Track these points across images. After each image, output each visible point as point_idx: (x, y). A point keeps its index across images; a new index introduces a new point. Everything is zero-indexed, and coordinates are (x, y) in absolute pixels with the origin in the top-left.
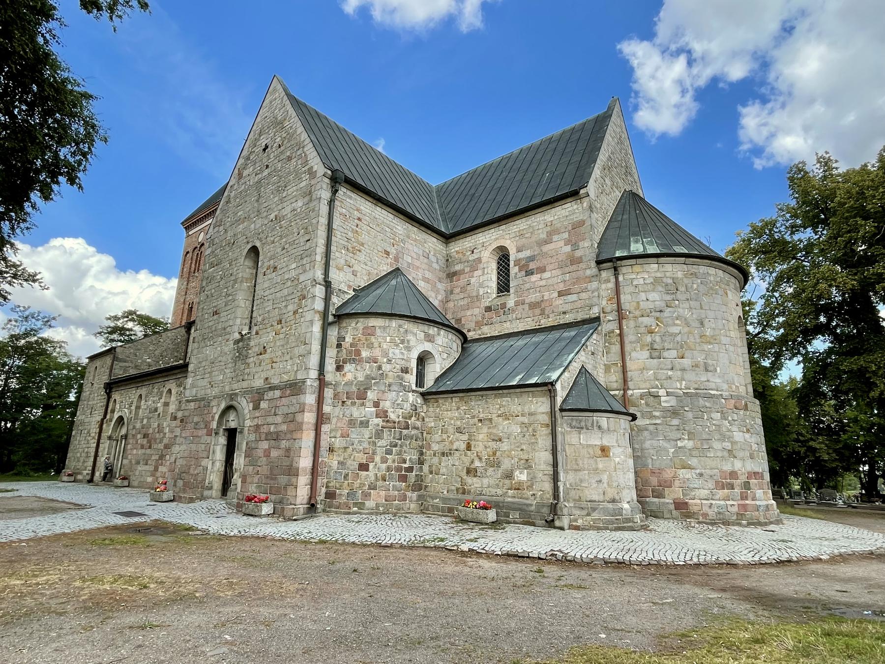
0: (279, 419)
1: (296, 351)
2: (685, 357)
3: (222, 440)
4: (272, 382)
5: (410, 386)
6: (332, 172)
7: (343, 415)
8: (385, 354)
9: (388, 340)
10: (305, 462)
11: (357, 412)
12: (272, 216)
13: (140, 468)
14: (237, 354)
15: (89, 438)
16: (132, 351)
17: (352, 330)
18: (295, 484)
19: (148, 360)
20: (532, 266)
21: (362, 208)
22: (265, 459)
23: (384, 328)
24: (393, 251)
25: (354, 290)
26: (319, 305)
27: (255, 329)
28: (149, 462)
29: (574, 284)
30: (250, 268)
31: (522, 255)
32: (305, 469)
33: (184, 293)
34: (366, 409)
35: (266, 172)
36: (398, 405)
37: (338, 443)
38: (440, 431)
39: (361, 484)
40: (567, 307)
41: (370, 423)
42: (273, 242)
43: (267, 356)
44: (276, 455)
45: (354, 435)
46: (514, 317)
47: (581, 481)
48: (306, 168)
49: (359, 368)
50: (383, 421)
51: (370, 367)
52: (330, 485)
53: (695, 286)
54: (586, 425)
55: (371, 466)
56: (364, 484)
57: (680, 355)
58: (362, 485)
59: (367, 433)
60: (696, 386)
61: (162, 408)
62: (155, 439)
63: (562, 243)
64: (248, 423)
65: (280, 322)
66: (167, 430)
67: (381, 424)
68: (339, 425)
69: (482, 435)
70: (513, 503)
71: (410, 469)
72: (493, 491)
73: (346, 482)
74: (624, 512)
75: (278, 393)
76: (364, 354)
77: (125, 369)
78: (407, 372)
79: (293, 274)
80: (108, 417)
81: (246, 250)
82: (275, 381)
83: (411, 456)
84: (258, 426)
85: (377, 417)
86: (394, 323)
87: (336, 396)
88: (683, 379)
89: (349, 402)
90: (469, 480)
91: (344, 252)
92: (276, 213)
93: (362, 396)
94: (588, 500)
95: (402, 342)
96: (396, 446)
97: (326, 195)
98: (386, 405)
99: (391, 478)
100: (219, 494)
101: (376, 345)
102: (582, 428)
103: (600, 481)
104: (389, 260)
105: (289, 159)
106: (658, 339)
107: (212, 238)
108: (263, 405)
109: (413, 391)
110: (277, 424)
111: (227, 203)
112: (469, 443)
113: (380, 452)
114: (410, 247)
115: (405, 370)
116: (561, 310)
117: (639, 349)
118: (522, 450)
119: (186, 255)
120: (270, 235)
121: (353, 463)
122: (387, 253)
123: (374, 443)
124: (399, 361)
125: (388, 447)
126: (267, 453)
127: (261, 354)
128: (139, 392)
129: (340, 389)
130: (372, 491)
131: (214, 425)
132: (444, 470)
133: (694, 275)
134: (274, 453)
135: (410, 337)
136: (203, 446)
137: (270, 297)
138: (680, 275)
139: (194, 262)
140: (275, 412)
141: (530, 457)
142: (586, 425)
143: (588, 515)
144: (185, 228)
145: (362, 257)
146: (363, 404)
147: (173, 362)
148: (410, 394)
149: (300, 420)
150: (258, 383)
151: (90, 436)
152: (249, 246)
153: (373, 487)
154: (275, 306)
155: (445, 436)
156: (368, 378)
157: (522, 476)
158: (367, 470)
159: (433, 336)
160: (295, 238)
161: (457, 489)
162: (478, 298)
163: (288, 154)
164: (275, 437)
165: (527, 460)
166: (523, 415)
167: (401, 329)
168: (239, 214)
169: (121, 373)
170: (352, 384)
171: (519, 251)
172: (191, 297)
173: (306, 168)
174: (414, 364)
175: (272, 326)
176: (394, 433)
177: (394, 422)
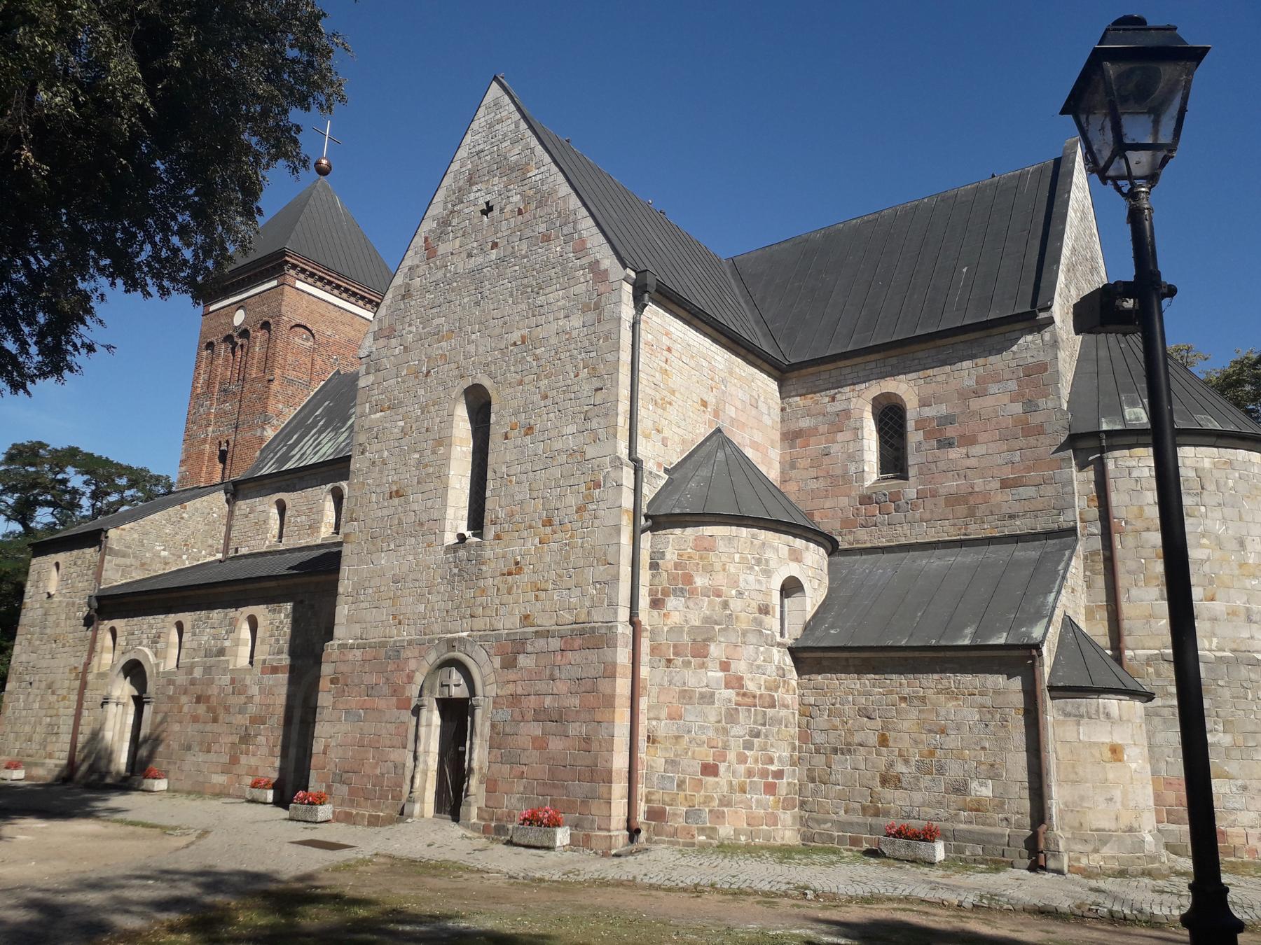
0: (561, 687)
1: (589, 574)
2: (1217, 596)
5: (773, 636)
6: (636, 273)
7: (670, 682)
8: (736, 583)
9: (737, 560)
10: (620, 762)
11: (694, 679)
12: (516, 336)
14: (456, 571)
16: (136, 536)
17: (677, 541)
18: (606, 796)
19: (164, 553)
20: (950, 432)
21: (672, 329)
22: (536, 753)
23: (730, 539)
24: (711, 399)
25: (666, 470)
26: (627, 501)
29: (1028, 469)
31: (928, 412)
32: (620, 770)
34: (709, 673)
35: (494, 254)
36: (759, 667)
37: (664, 728)
38: (826, 713)
39: (706, 797)
40: (1017, 508)
41: (717, 696)
42: (520, 383)
43: (523, 578)
44: (561, 747)
45: (692, 716)
46: (918, 516)
47: (1082, 798)
48: (585, 261)
49: (691, 604)
50: (738, 694)
51: (709, 603)
52: (653, 797)
53: (1231, 483)
54: (1087, 712)
55: (722, 768)
56: (712, 798)
57: (1209, 594)
58: (708, 799)
60: (1234, 646)
63: (1006, 399)
65: (548, 522)
66: (255, 690)
67: (734, 698)
68: (662, 699)
69: (908, 723)
70: (969, 832)
71: (779, 774)
72: (932, 812)
73: (682, 794)
74: (1147, 847)
75: (555, 643)
76: (700, 581)
77: (125, 569)
78: (767, 613)
79: (571, 443)
82: (546, 622)
84: (515, 699)
85: (727, 687)
86: (744, 531)
87: (654, 650)
88: (1214, 635)
89: (679, 661)
90: (888, 793)
91: (651, 408)
92: (523, 332)
93: (700, 652)
94: (1094, 827)
95: (758, 562)
96: (758, 735)
97: (627, 311)
98: (740, 667)
99: (754, 789)
100: (439, 808)
101: (718, 566)
102: (1082, 716)
103: (1111, 799)
105: (546, 238)
107: (373, 357)
108: (522, 660)
109: (779, 645)
110: (561, 694)
111: (403, 297)
112: (883, 735)
113: (735, 746)
115: (765, 610)
116: (1006, 510)
117: (1142, 583)
118: (983, 748)
120: (512, 368)
121: (692, 762)
122: (704, 404)
123: (725, 731)
124: (754, 595)
125: (747, 737)
126: (540, 744)
127: (510, 574)
129: (662, 639)
130: (726, 809)
132: (839, 777)
133: (1230, 464)
134: (555, 744)
135: (769, 554)
136: (392, 728)
138: (1207, 463)
140: (551, 675)
141: (998, 760)
142: (1087, 712)
143: (1096, 851)
145: (672, 413)
146: (703, 666)
147: (205, 557)
148: (775, 650)
149: (608, 691)
150: (508, 623)
152: (468, 382)
153: (726, 803)
154: (535, 494)
155: (837, 722)
156: (707, 623)
157: (983, 790)
158: (716, 774)
159: (801, 552)
161: (864, 809)
162: (846, 478)
163: (542, 228)
164: (555, 716)
165: (992, 766)
166: (981, 694)
167: (756, 542)
168: (435, 322)
170: (682, 632)
171: (924, 403)
173: (585, 261)
175: (531, 527)
176: (755, 715)
177: (754, 697)
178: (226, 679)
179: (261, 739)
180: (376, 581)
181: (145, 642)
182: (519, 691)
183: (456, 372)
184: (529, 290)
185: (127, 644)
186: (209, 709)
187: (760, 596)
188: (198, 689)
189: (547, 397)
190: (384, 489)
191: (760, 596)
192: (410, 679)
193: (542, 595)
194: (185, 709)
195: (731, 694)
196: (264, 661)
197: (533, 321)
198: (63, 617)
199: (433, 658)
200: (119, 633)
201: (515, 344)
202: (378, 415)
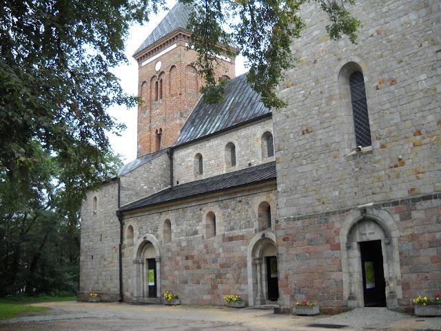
3: (356, 253)
4: (422, 192)
13: (188, 288)
15: (106, 263)
27: (376, 144)
28: (201, 281)
30: (344, 84)
33: (148, 122)
42: (381, 56)
61: (204, 231)
62: (205, 261)
64: (395, 234)
65: (419, 133)
66: (221, 250)
77: (129, 196)
79: (425, 85)
80: (126, 242)
81: (339, 68)
84: (413, 237)
92: (377, 28)
108: (415, 214)
119: (142, 86)
127: (396, 166)
128: (164, 217)
131: (343, 239)
136: (329, 261)
137: (393, 110)
139: (154, 90)
144: (138, 60)
147: (163, 188)
151: (105, 260)
152: (343, 63)
154: (404, 118)
160: (416, 50)
169: (127, 200)
172: (156, 125)
178: (202, 246)
179: (229, 275)
180: (303, 182)
181: (150, 231)
182: (416, 232)
183: (334, 58)
184: (376, 5)
185: (140, 233)
186: (194, 262)
188: (186, 253)
189: (402, 61)
190: (296, 130)
192: (337, 233)
193: (420, 175)
194: (180, 263)
196: (224, 235)
197: (382, 21)
198: (103, 223)
199: (351, 219)
200: (134, 229)
201: (372, 35)
202: (286, 90)
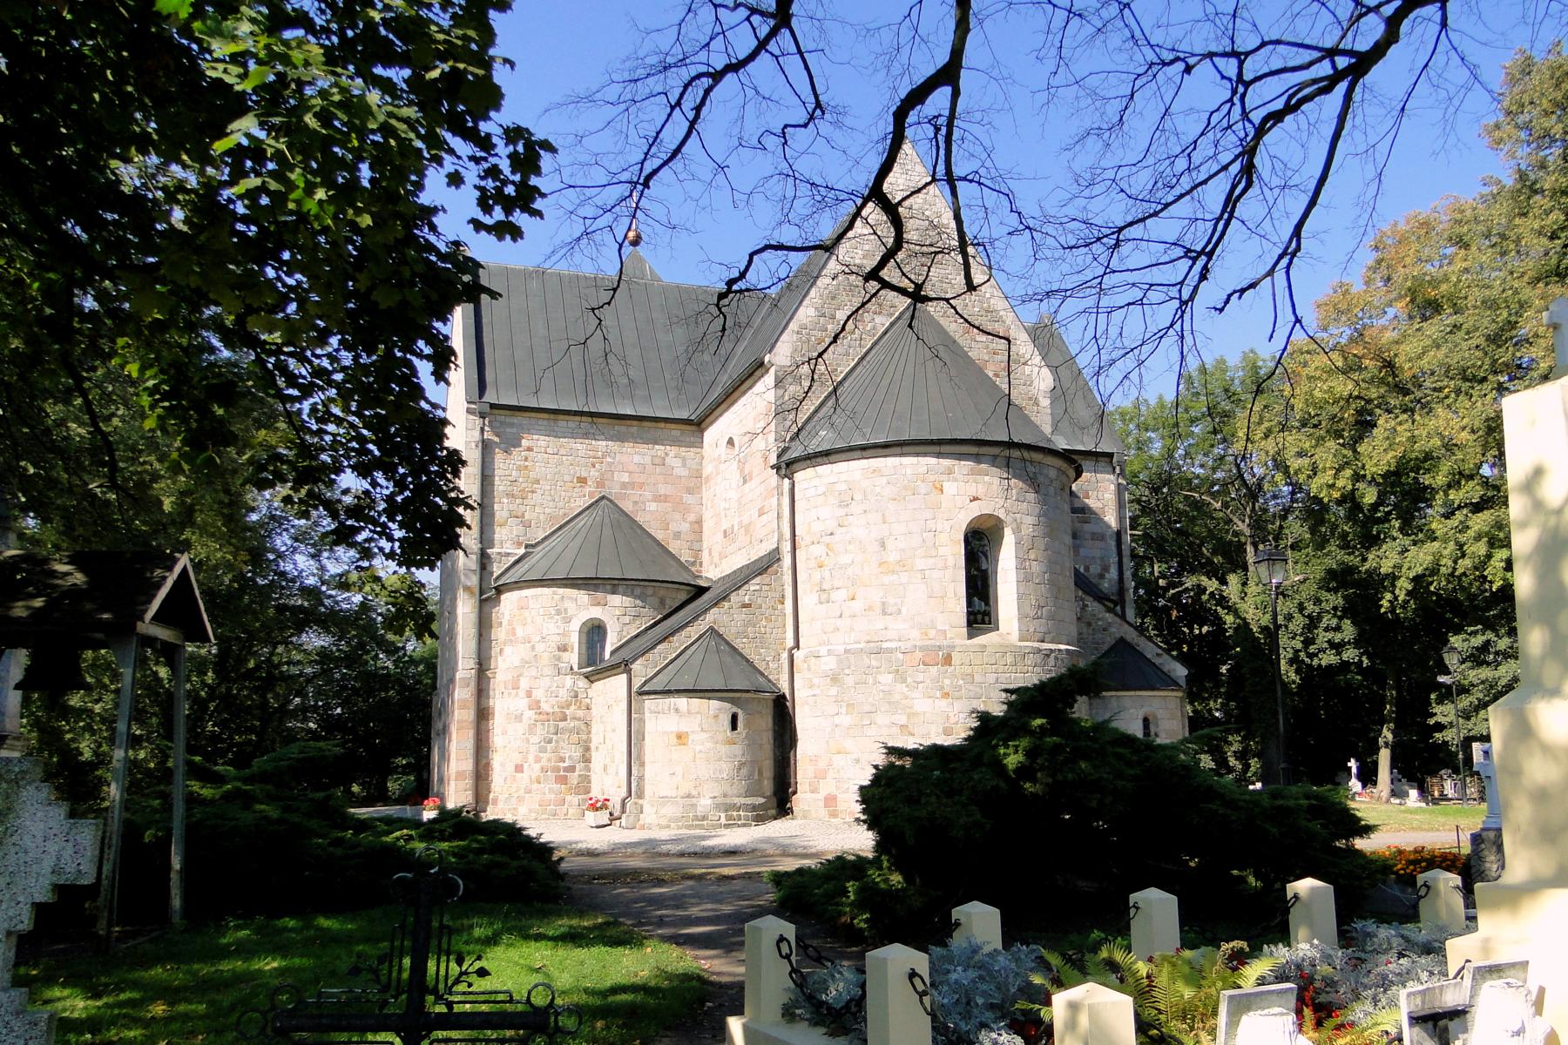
23: (536, 596)
55: (526, 766)
59: (521, 728)
67: (534, 717)
71: (572, 769)
76: (520, 633)
78: (565, 650)
83: (572, 753)
91: (505, 501)
95: (558, 612)
96: (550, 742)
98: (538, 694)
101: (529, 620)
104: (587, 490)
106: (827, 575)
109: (576, 673)
113: (533, 749)
114: (624, 459)
115: (563, 648)
122: (583, 481)
123: (528, 741)
135: (569, 605)
174: (574, 639)
187: (558, 638)
191: (557, 638)
195: (531, 714)
